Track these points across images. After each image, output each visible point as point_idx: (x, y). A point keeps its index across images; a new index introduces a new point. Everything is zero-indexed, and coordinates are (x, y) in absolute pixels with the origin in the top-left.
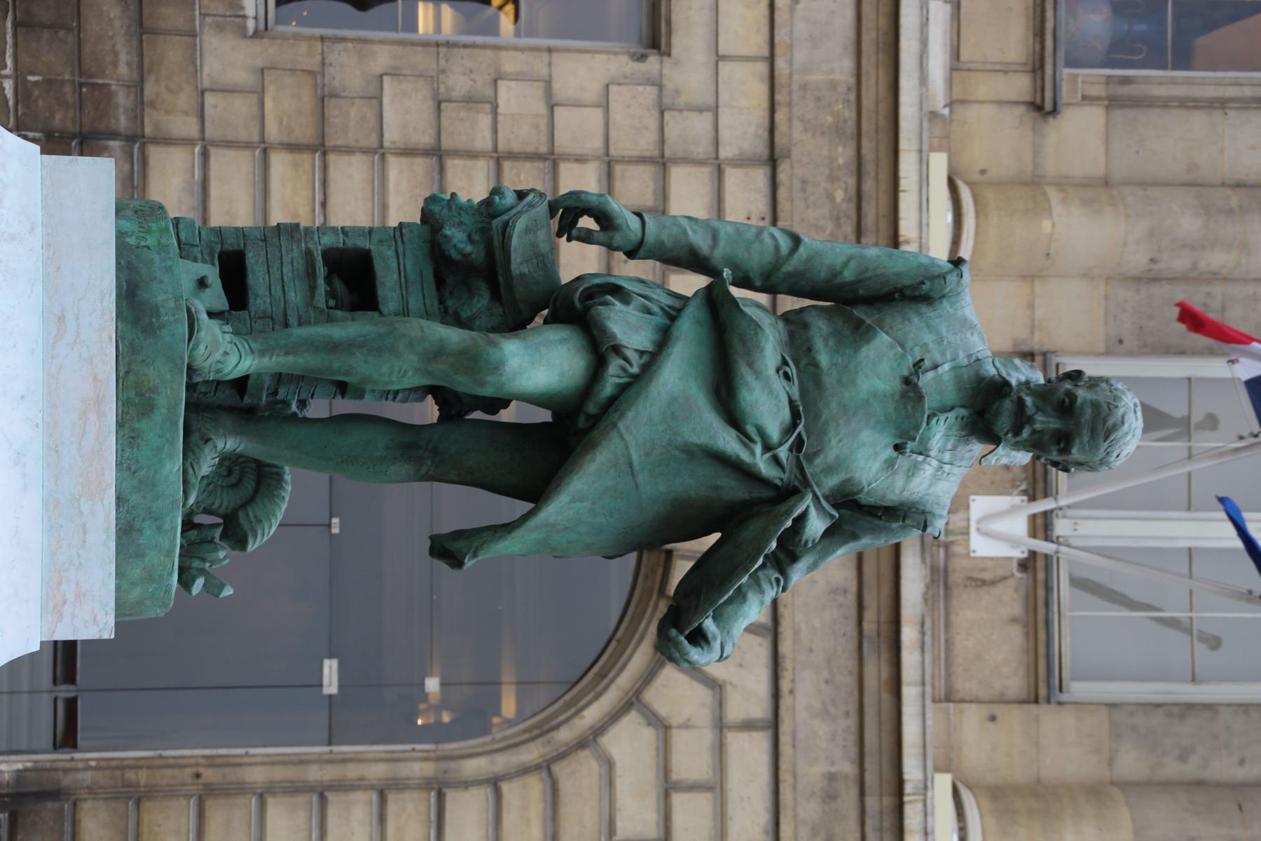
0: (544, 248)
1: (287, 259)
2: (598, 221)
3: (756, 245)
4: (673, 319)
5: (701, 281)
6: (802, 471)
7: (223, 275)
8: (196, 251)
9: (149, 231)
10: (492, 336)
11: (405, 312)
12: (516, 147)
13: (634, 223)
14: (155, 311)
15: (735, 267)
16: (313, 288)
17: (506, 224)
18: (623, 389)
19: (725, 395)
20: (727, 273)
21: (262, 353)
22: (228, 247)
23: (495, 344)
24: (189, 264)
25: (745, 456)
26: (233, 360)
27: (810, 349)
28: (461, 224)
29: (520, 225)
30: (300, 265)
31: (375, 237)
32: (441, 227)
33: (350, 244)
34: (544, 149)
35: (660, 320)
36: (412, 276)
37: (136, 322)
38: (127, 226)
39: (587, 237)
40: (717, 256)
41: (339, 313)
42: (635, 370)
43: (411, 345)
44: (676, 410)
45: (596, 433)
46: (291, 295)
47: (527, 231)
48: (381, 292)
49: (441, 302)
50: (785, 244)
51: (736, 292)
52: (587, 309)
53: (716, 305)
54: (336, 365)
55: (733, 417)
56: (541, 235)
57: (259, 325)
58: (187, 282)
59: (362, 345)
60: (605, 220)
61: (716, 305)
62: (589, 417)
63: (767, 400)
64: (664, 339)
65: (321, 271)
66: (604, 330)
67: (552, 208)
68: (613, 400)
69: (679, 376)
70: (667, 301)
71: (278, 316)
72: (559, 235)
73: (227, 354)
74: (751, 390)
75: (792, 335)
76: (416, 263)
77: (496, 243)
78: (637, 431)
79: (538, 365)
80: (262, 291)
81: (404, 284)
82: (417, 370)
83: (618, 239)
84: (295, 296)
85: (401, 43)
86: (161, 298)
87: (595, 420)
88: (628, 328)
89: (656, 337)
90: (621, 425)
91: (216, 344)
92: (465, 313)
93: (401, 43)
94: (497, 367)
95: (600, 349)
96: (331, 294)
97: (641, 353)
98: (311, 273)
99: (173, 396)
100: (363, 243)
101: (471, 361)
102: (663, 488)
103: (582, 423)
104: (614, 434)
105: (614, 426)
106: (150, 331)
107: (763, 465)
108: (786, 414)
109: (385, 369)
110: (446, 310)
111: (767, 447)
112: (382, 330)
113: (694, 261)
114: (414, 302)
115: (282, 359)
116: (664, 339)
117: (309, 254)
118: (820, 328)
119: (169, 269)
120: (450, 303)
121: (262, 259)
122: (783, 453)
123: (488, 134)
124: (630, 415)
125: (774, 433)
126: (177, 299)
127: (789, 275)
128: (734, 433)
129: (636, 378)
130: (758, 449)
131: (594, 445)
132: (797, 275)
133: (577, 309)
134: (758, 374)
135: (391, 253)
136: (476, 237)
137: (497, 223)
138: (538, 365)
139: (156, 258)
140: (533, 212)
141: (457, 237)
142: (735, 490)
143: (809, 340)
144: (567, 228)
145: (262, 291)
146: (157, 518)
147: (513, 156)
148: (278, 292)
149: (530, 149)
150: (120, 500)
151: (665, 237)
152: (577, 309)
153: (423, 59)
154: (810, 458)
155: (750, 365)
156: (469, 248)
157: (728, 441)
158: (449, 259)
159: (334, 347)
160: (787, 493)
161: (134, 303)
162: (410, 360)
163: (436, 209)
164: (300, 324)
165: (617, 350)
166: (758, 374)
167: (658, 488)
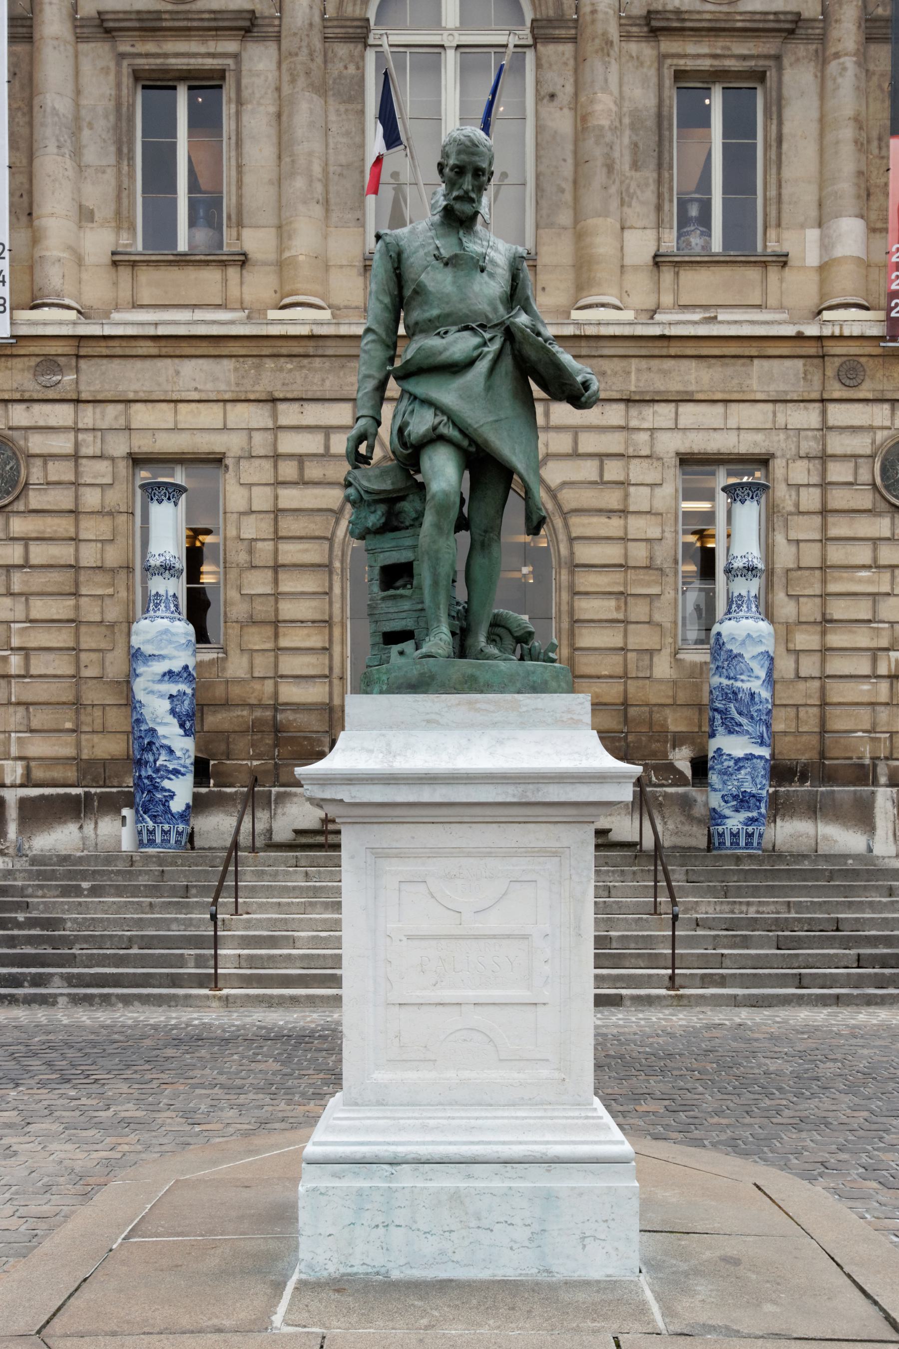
0: (377, 471)
1: (387, 610)
2: (361, 442)
3: (372, 353)
4: (415, 398)
5: (392, 383)
6: (496, 325)
7: (396, 643)
8: (384, 657)
9: (379, 679)
10: (428, 498)
11: (414, 547)
12: (272, 530)
13: (362, 422)
14: (422, 675)
15: (384, 365)
16: (402, 596)
17: (367, 492)
18: (455, 425)
19: (455, 368)
20: (389, 368)
21: (439, 621)
22: (381, 640)
23: (433, 497)
24: (392, 660)
25: (490, 357)
26: (443, 636)
27: (430, 320)
28: (365, 517)
29: (365, 483)
30: (390, 603)
31: (374, 564)
32: (368, 528)
33: (377, 577)
34: (272, 516)
35: (417, 405)
36: (394, 544)
37: (428, 684)
38: (376, 689)
39: (371, 448)
40: (379, 375)
41: (415, 582)
42: (445, 418)
43: (434, 542)
44: (466, 395)
45: (479, 441)
46: (406, 608)
47: (369, 481)
48: (403, 560)
49: (407, 528)
50: (370, 337)
51: (398, 363)
52: (412, 446)
53: (406, 374)
54: (445, 583)
55: (470, 363)
56: (371, 473)
57: (422, 624)
58: (402, 660)
59: (435, 569)
60: (361, 438)
61: (406, 374)
62: (470, 445)
63: (459, 345)
64: (427, 402)
65: (392, 592)
66: (424, 436)
67: (356, 467)
68: (461, 431)
69: (447, 393)
70: (405, 402)
71: (417, 614)
72: (369, 464)
73: (440, 639)
74: (454, 353)
75: (422, 331)
76: (387, 541)
77: (376, 497)
78: (478, 417)
79: (443, 472)
80: (404, 622)
81: (398, 548)
82: (447, 539)
83: (371, 430)
84: (406, 605)
85: (225, 586)
86: (415, 672)
87: (472, 441)
88: (422, 423)
89: (426, 407)
90: (476, 426)
91: (436, 644)
92: (414, 515)
93: (225, 586)
94: (446, 494)
95: (435, 438)
96: (404, 586)
97: (436, 415)
98: (394, 597)
99: (464, 665)
100: (377, 571)
101: (442, 509)
102: (507, 404)
103: (473, 449)
104: (480, 430)
105: (475, 430)
106: (432, 677)
107: (494, 347)
108: (466, 334)
109: (447, 556)
110: (412, 525)
111: (485, 344)
112: (426, 558)
113: (382, 386)
114: (408, 542)
115: (442, 611)
116: (427, 402)
117: (383, 599)
118: (417, 315)
119: (400, 668)
120: (407, 524)
121: (387, 623)
122: (487, 336)
123: (266, 543)
124: (469, 421)
125: (477, 340)
126: (415, 664)
127: (387, 334)
128: (477, 363)
129: (449, 418)
130: (486, 349)
131: (486, 442)
132: (387, 329)
133: (410, 454)
134: (445, 349)
135: (381, 555)
136: (373, 509)
137: (366, 497)
138: (443, 472)
139: (393, 674)
140: (359, 477)
141: (374, 519)
142: (507, 363)
143: (424, 321)
144: (365, 460)
145: (404, 622)
146: (528, 674)
147: (276, 531)
148: (404, 615)
149: (272, 523)
150: (519, 692)
151: (369, 405)
152: (410, 454)
153: (233, 574)
154: (489, 320)
155: (441, 353)
156: (379, 513)
157: (483, 366)
158: (385, 524)
159: (435, 583)
160: (509, 334)
161: (418, 685)
162: (442, 543)
163: (357, 531)
164: (422, 602)
165: (435, 428)
166: (445, 349)
167: (508, 407)
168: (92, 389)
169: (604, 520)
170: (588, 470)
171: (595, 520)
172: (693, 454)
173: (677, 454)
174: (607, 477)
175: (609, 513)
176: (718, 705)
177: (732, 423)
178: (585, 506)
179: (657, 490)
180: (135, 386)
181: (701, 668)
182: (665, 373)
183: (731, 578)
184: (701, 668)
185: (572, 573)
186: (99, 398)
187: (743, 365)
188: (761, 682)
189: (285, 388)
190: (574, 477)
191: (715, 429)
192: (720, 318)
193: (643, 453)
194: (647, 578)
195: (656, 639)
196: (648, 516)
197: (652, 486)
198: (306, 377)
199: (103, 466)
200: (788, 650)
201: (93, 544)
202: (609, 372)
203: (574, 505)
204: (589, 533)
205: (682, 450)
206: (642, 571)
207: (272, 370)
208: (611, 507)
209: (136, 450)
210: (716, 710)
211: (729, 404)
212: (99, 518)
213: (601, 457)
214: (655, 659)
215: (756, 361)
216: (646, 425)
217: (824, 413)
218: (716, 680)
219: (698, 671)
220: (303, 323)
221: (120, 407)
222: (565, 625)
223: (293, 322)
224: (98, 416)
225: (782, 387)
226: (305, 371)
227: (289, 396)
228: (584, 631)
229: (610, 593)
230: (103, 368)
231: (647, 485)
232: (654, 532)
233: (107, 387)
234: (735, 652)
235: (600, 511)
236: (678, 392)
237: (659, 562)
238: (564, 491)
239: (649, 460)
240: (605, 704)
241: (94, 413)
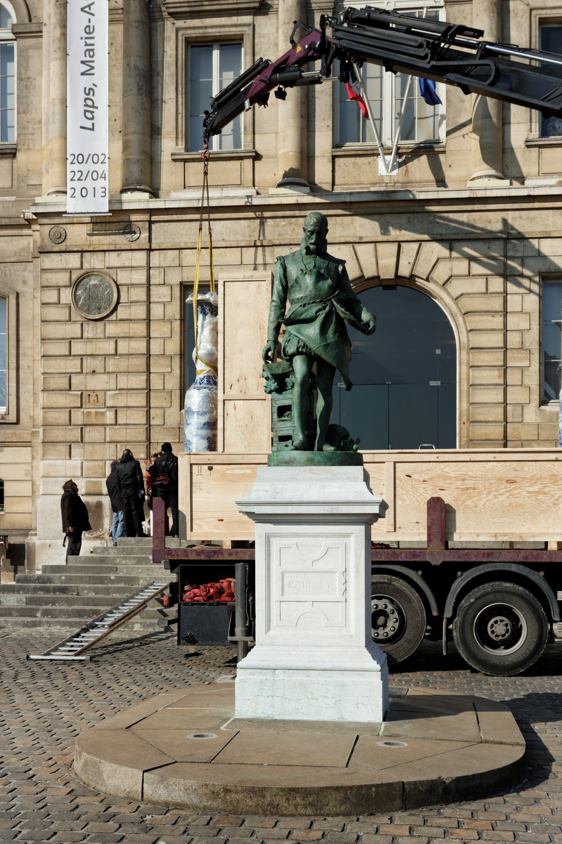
168: (159, 242)
169: (490, 318)
172: (551, 272)
174: (491, 290)
175: (493, 313)
178: (477, 309)
180: (185, 239)
182: (531, 219)
186: (163, 247)
189: (280, 237)
194: (519, 355)
196: (520, 315)
198: (294, 230)
199: (165, 290)
201: (158, 340)
202: (493, 220)
206: (516, 351)
207: (272, 226)
208: (495, 309)
209: (185, 279)
212: (162, 323)
214: (525, 410)
216: (518, 255)
219: (555, 417)
221: (177, 252)
224: (162, 258)
226: (293, 226)
228: (477, 392)
230: (166, 228)
232: (524, 325)
233: (167, 240)
236: (540, 232)
237: (527, 345)
238: (463, 299)
240: (491, 440)
241: (160, 257)
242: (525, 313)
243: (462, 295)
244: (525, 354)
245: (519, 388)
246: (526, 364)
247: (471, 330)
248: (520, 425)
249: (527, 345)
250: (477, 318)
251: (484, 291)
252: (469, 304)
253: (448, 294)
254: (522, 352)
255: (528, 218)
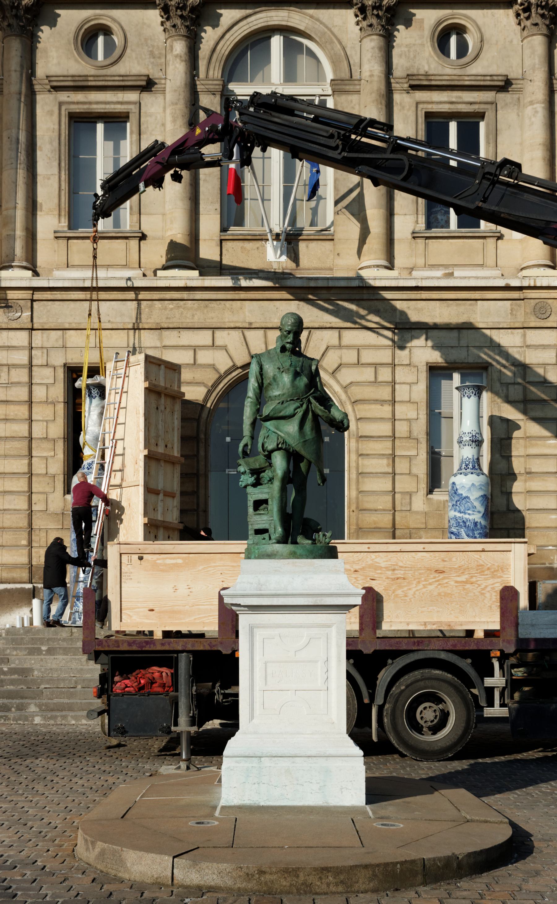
169: (378, 407)
170: (368, 374)
171: (373, 406)
173: (427, 363)
174: (380, 379)
175: (382, 402)
176: (454, 530)
177: (463, 343)
179: (414, 387)
181: (444, 504)
183: (462, 446)
184: (444, 504)
185: (357, 441)
187: (471, 305)
188: (481, 515)
189: (168, 321)
190: (359, 379)
191: (452, 347)
192: (456, 274)
193: (405, 362)
194: (408, 444)
195: (415, 485)
197: (410, 384)
198: (182, 313)
200: (502, 492)
203: (359, 397)
204: (368, 416)
205: (431, 361)
206: (404, 440)
207: (160, 309)
210: (452, 533)
211: (462, 331)
213: (376, 366)
215: (479, 302)
217: (524, 336)
218: (453, 514)
220: (181, 278)
222: (354, 476)
223: (174, 278)
225: (496, 320)
226: (181, 309)
227: (171, 326)
229: (383, 455)
231: (408, 383)
234: (464, 495)
235: (376, 401)
237: (415, 434)
238: (353, 388)
239: (408, 368)
242: (413, 403)
243: (351, 383)
244: (413, 443)
245: (408, 476)
246: (413, 453)
247: (360, 419)
248: (408, 513)
249: (415, 434)
250: (366, 407)
251: (373, 380)
252: (358, 392)
253: (338, 382)
254: (410, 441)
255: (416, 309)
